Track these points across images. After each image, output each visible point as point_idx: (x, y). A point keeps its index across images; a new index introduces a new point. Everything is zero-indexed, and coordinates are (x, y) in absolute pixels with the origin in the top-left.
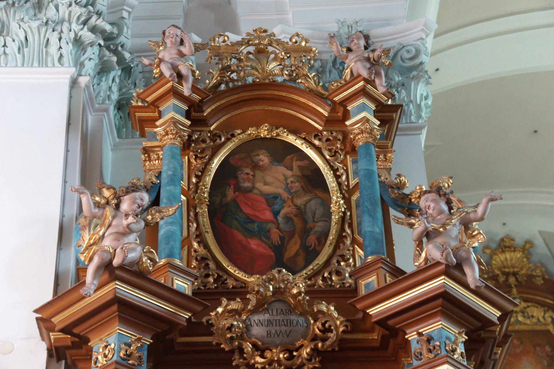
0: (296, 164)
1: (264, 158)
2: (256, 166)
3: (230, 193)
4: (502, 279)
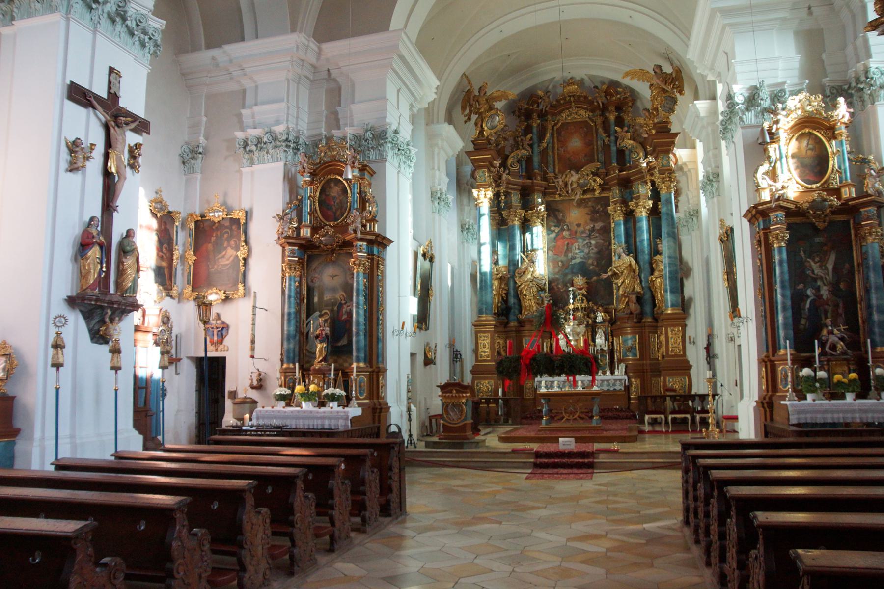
0: (341, 186)
1: (332, 185)
2: (330, 188)
3: (324, 197)
4: (568, 99)
